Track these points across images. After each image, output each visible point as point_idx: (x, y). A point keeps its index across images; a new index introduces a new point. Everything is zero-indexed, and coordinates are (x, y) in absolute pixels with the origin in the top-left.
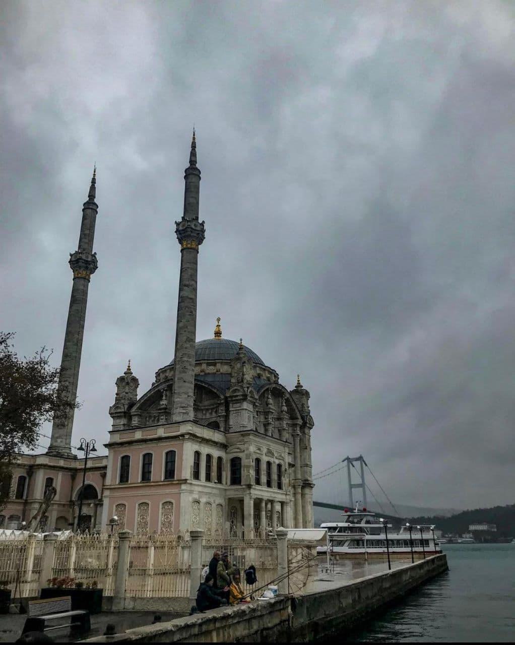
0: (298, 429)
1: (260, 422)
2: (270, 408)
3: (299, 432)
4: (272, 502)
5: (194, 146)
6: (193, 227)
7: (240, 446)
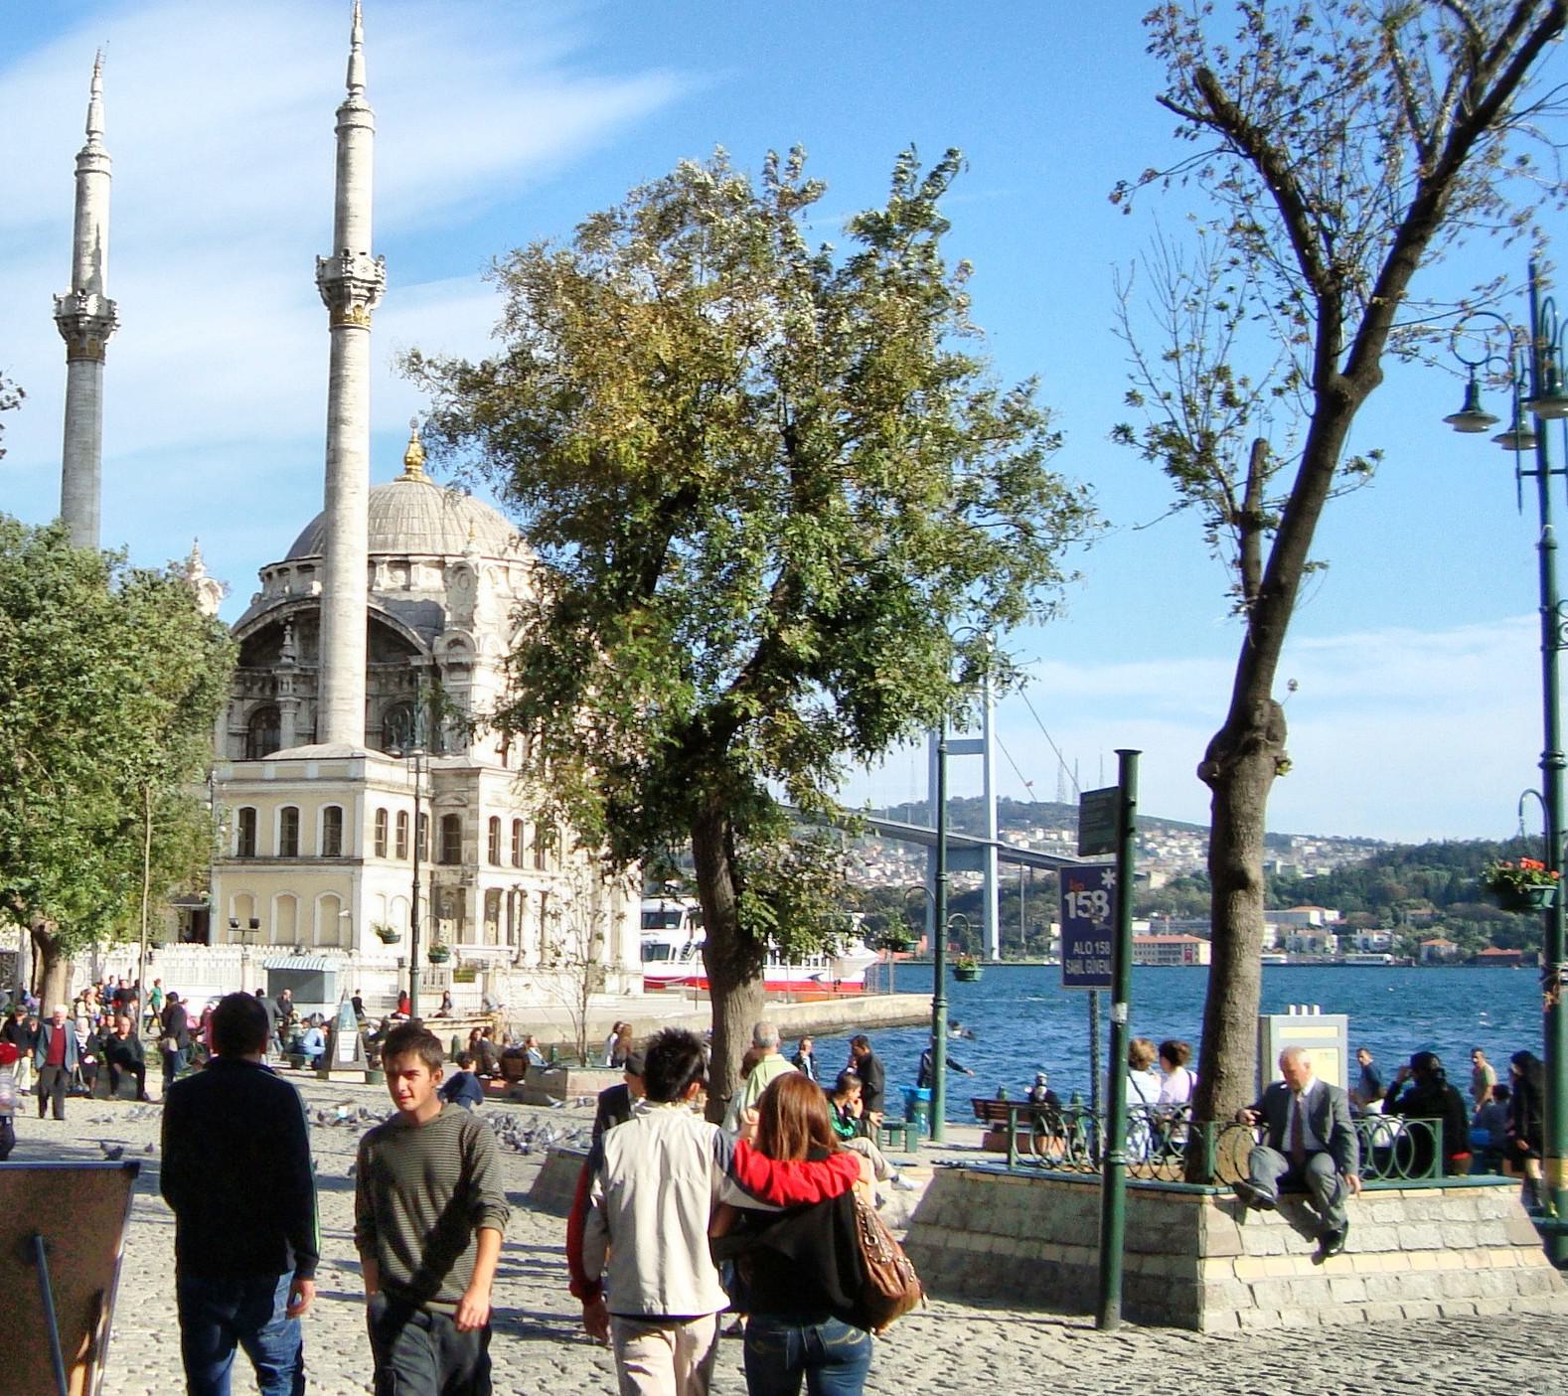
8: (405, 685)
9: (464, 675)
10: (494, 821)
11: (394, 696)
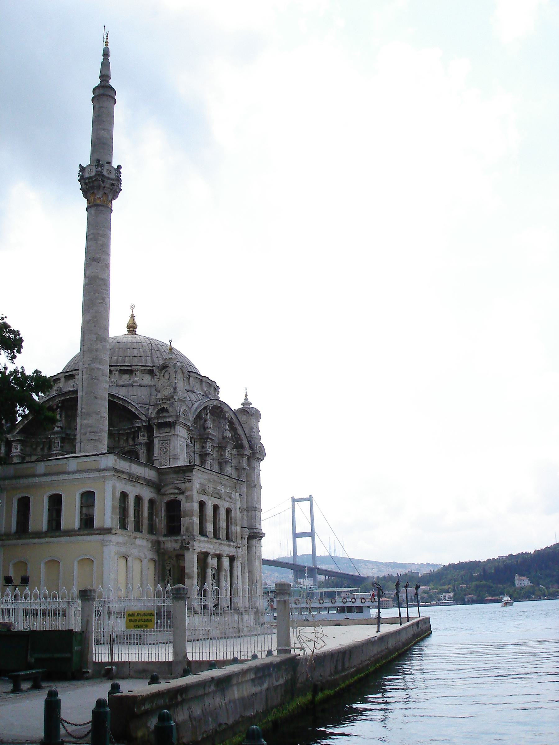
0: (245, 460)
1: (194, 452)
2: (209, 434)
3: (245, 466)
4: (219, 557)
5: (106, 54)
6: (105, 173)
7: (179, 485)
8: (130, 441)
9: (167, 430)
10: (202, 505)
11: (124, 448)
